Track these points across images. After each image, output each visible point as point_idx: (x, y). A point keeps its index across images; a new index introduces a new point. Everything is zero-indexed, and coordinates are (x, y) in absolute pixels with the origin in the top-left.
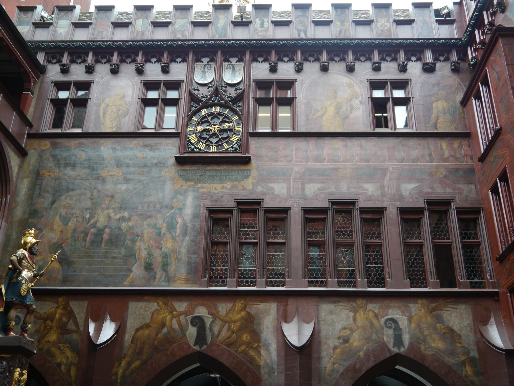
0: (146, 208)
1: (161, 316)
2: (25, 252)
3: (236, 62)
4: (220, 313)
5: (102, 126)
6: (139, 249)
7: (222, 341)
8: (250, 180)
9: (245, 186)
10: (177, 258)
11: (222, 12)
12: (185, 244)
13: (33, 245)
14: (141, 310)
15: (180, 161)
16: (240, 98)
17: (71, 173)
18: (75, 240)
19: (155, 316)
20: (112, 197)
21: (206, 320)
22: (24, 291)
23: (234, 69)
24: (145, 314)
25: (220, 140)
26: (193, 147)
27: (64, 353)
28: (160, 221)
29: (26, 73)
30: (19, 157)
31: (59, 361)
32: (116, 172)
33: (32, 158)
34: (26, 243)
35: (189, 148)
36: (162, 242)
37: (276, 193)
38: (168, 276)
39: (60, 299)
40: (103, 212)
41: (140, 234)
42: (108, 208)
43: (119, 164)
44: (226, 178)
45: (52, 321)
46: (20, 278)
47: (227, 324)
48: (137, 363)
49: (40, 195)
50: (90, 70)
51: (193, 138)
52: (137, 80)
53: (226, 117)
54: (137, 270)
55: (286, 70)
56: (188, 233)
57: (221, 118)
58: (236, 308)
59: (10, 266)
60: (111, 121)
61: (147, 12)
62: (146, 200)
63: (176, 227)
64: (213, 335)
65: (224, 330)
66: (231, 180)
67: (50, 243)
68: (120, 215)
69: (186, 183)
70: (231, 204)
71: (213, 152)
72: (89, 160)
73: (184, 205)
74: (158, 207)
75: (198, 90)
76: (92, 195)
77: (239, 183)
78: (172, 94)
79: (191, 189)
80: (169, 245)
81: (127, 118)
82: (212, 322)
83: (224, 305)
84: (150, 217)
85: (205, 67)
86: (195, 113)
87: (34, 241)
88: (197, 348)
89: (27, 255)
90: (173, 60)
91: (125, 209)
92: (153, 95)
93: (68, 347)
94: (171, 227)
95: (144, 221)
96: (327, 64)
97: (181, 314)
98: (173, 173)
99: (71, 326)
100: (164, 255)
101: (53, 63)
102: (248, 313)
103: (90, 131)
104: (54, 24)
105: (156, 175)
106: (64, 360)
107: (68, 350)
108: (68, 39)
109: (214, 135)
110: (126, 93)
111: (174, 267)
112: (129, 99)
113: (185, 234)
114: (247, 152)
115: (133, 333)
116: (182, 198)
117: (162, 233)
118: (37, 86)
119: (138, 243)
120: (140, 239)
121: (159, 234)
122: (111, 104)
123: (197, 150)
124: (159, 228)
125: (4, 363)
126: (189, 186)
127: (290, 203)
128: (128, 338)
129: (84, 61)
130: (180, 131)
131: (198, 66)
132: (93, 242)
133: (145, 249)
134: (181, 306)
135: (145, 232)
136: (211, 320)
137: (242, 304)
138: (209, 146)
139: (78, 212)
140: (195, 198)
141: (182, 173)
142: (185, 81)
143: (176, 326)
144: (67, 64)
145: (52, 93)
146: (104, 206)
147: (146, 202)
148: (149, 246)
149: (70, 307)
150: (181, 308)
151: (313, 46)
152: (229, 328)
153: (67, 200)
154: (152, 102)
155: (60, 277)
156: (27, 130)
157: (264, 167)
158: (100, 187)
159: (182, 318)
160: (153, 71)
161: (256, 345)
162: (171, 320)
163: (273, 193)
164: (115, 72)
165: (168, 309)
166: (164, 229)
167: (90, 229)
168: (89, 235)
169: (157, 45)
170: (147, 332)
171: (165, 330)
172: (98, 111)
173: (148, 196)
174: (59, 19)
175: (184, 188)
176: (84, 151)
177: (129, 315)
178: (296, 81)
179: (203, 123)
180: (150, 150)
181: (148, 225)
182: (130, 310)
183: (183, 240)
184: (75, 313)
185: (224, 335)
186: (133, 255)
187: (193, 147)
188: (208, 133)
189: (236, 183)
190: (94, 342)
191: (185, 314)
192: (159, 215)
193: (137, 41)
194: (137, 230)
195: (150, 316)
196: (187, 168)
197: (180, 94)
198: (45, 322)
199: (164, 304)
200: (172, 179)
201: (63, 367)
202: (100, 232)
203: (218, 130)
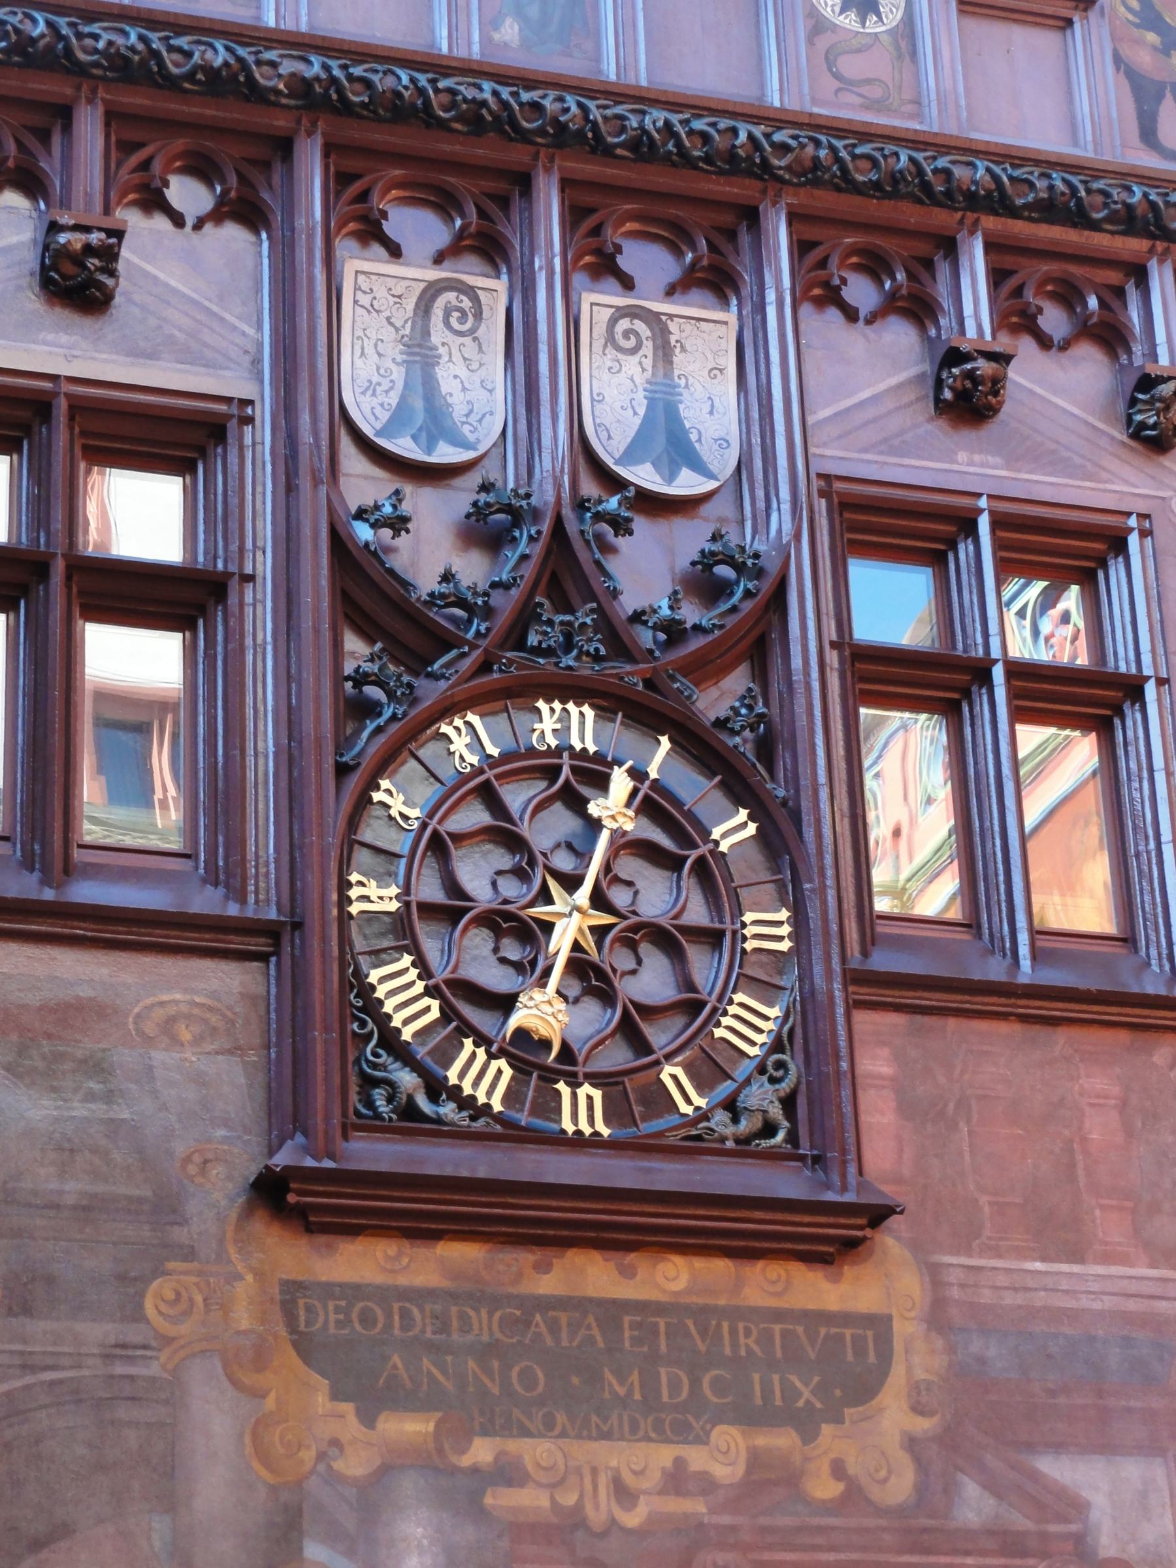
8: (893, 1416)
26: (407, 1079)
35: (369, 1083)
37: (1107, 1546)
69: (368, 1419)
71: (578, 1142)
77: (809, 1435)
98: (243, 1318)
123: (448, 1110)
142: (264, 413)
157: (986, 1296)
163: (1081, 1545)
175: (355, 1465)
189: (783, 1440)
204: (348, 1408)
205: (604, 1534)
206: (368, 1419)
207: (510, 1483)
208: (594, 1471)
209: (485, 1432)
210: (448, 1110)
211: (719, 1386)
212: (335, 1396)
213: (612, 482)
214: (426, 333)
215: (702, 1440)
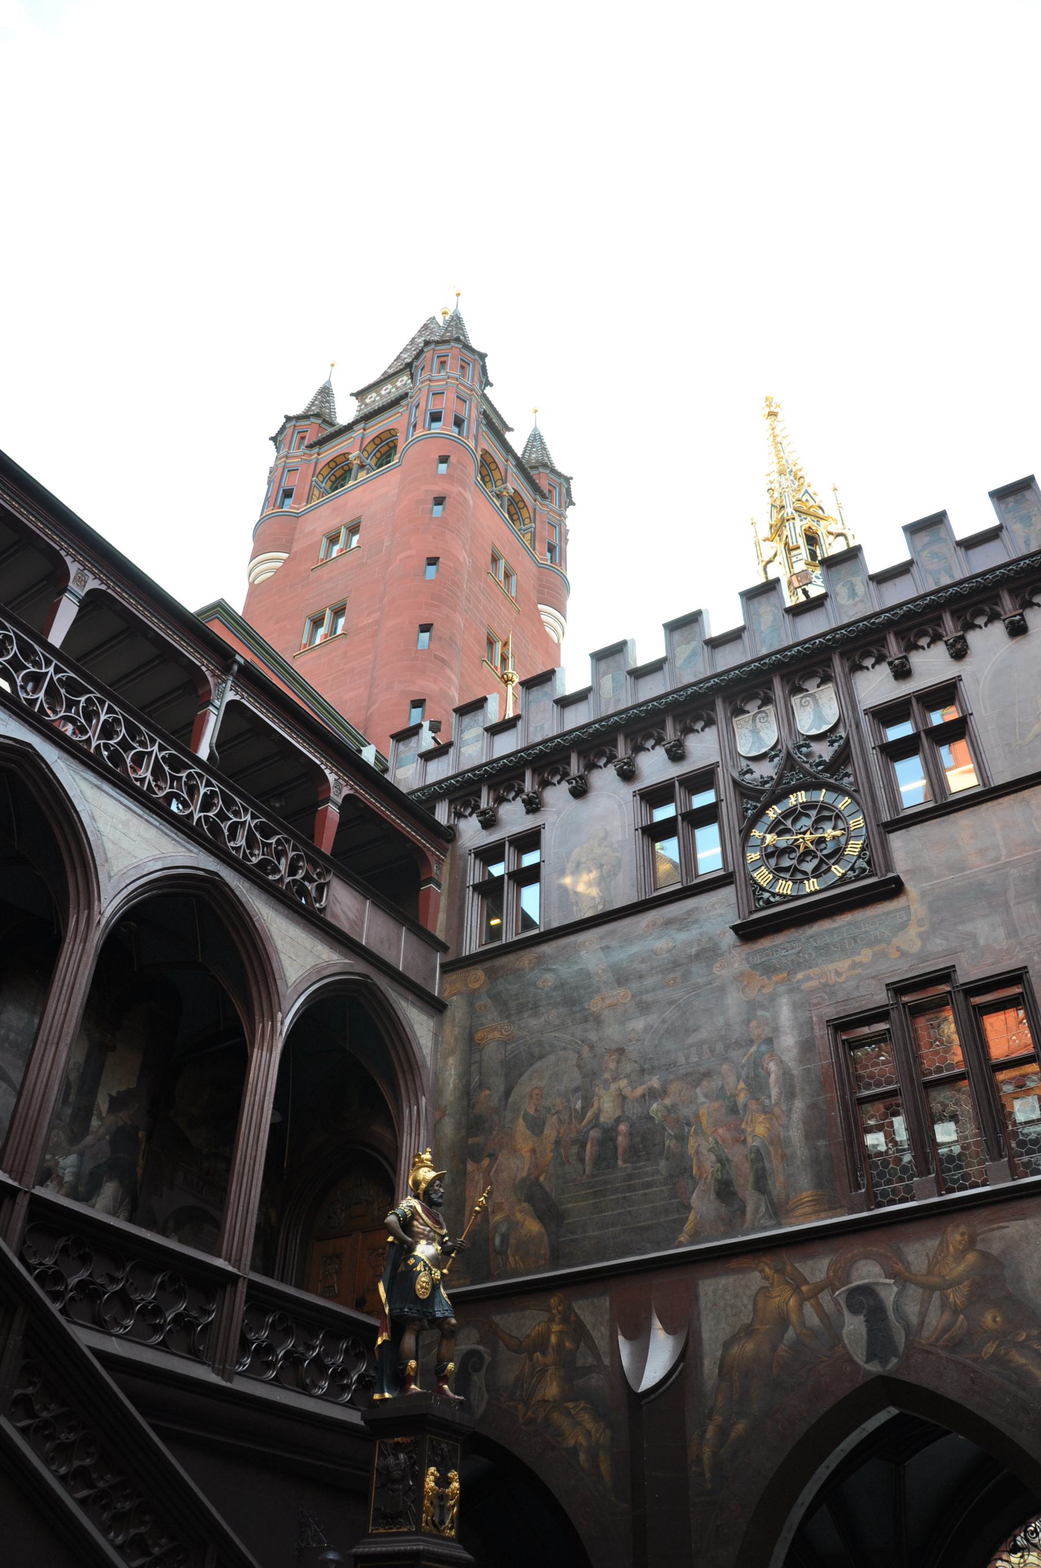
2: (415, 1203)
4: (914, 1269)
5: (575, 908)
6: (697, 1153)
7: (933, 1339)
8: (913, 932)
9: (904, 947)
10: (784, 1156)
11: (763, 599)
12: (796, 1116)
13: (431, 1183)
14: (728, 1297)
15: (748, 932)
16: (843, 757)
17: (533, 1022)
18: (562, 1164)
20: (621, 1051)
21: (883, 1293)
22: (422, 1288)
23: (816, 702)
25: (822, 862)
26: (766, 895)
27: (579, 1424)
28: (731, 1079)
29: (418, 850)
30: (431, 1016)
31: (572, 1442)
32: (620, 994)
33: (457, 1009)
34: (417, 1183)
35: (759, 899)
38: (772, 1203)
39: (553, 1301)
40: (607, 1088)
41: (692, 1120)
42: (615, 1079)
44: (855, 942)
45: (544, 1353)
46: (412, 1261)
47: (937, 1294)
48: (740, 1427)
49: (481, 1086)
50: (533, 806)
51: (763, 876)
52: (626, 792)
54: (702, 1204)
55: (932, 665)
56: (797, 1090)
57: (813, 813)
58: (951, 1248)
59: (390, 1239)
61: (617, 657)
62: (690, 1041)
63: (768, 1084)
64: (907, 1327)
65: (931, 1308)
66: (871, 944)
67: (514, 1180)
68: (644, 1086)
69: (770, 979)
70: (881, 997)
71: (812, 894)
72: (562, 985)
73: (776, 1030)
74: (719, 1047)
75: (750, 771)
76: (580, 1057)
77: (889, 943)
78: (703, 799)
79: (782, 989)
80: (761, 1130)
81: (620, 877)
82: (899, 1294)
83: (917, 1246)
84: (707, 1074)
85: (754, 720)
86: (754, 822)
87: (433, 1174)
88: (874, 1368)
89: (419, 1208)
90: (688, 730)
91: (653, 1070)
92: (664, 813)
93: (585, 1408)
94: (757, 1084)
95: (695, 1087)
96: (1018, 617)
97: (819, 1289)
100: (753, 1155)
101: (466, 817)
102: (985, 1256)
104: (455, 743)
105: (701, 981)
106: (581, 1439)
107: (586, 1416)
109: (808, 852)
110: (608, 828)
111: (782, 1179)
112: (617, 837)
113: (790, 1094)
114: (889, 867)
115: (719, 1354)
116: (767, 1014)
117: (740, 1105)
118: (446, 868)
119: (692, 1142)
121: (733, 1110)
122: (584, 859)
123: (777, 898)
126: (776, 983)
127: (1022, 956)
128: (709, 1366)
129: (521, 791)
130: (731, 869)
132: (598, 1160)
133: (710, 1150)
134: (817, 1268)
135: (703, 1111)
136: (895, 1289)
137: (963, 1234)
138: (801, 881)
139: (558, 1101)
140: (796, 1007)
143: (813, 1319)
144: (491, 809)
145: (475, 874)
146: (607, 1075)
147: (691, 1046)
148: (717, 1142)
149: (577, 1316)
150: (817, 1273)
151: (975, 591)
152: (944, 1304)
153: (534, 1082)
155: (545, 1250)
158: (592, 1036)
159: (825, 1297)
160: (654, 766)
161: (1023, 1336)
164: (580, 792)
165: (788, 1283)
166: (742, 1095)
167: (588, 1132)
168: (589, 1146)
170: (750, 1346)
171: (790, 1334)
173: (694, 1031)
176: (550, 970)
177: (703, 1313)
178: (959, 678)
181: (706, 1096)
182: (703, 1300)
183: (790, 1110)
184: (588, 1327)
185: (934, 1323)
187: (766, 895)
188: (792, 856)
190: (634, 1388)
191: (830, 1285)
192: (725, 1067)
193: (608, 718)
194: (686, 1111)
195: (750, 1307)
196: (766, 943)
197: (718, 794)
198: (531, 1360)
199: (777, 1271)
201: (582, 1457)
202: (609, 1135)
203: (812, 843)
206: (770, 979)
211: (862, 939)
212: (762, 975)
215: (859, 954)
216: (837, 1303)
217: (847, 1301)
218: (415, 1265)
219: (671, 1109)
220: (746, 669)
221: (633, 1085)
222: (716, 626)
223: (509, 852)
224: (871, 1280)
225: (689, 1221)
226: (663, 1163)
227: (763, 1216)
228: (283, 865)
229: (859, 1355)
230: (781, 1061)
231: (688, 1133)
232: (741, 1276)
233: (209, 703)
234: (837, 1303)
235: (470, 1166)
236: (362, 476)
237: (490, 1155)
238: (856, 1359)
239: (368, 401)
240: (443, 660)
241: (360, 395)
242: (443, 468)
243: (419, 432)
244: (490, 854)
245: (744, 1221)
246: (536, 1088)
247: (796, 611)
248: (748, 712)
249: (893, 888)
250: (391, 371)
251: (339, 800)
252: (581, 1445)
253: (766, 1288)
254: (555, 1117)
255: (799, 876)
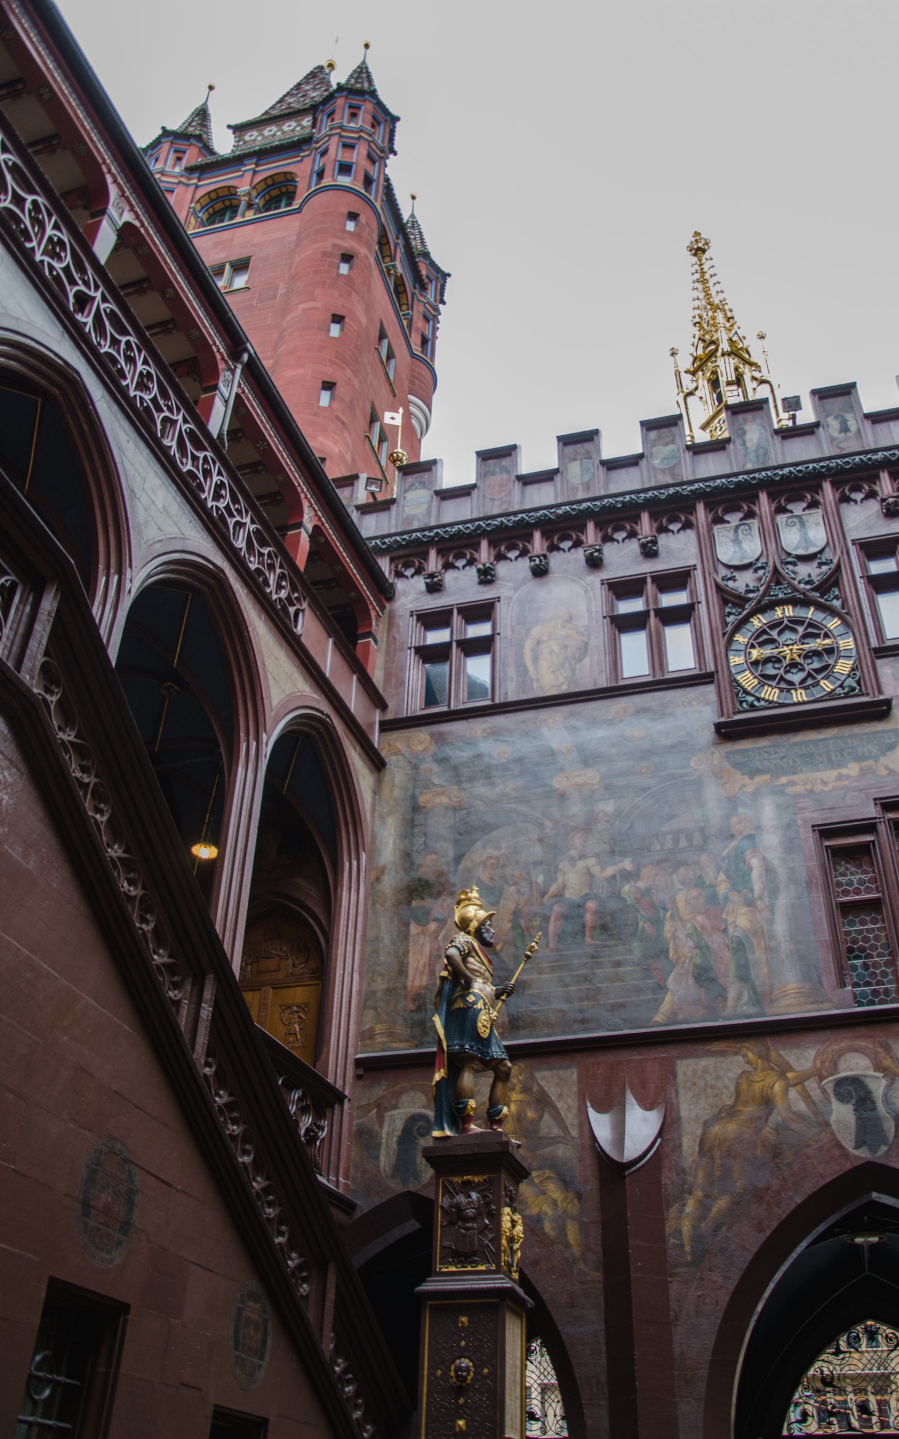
0: (669, 845)
1: (757, 1087)
3: (804, 510)
5: (535, 685)
6: (674, 937)
9: (891, 766)
13: (482, 923)
15: (728, 732)
16: (832, 582)
19: (744, 1087)
22: (484, 1026)
23: (803, 524)
24: (720, 1085)
25: (809, 675)
26: (750, 699)
29: (362, 600)
31: (535, 1211)
35: (741, 702)
36: (724, 916)
38: (755, 993)
41: (669, 906)
42: (583, 857)
43: (588, 759)
44: (842, 755)
46: (471, 998)
48: (722, 1203)
50: (487, 577)
51: (747, 680)
53: (810, 625)
57: (801, 629)
60: (553, 672)
61: (588, 446)
62: (665, 829)
66: (858, 759)
69: (752, 778)
70: (871, 811)
71: (799, 704)
74: (697, 838)
75: (733, 578)
77: (876, 761)
80: (743, 921)
81: (587, 661)
82: (889, 1087)
84: (685, 864)
86: (738, 628)
88: (863, 1154)
91: (623, 854)
99: (548, 1127)
101: (407, 577)
103: (511, 698)
106: (547, 1208)
108: (433, 523)
109: (794, 665)
114: (880, 692)
115: (699, 1132)
119: (668, 927)
120: (671, 915)
121: (713, 899)
122: (545, 638)
123: (763, 703)
124: (711, 886)
125: (474, 1195)
128: (689, 1144)
130: (711, 668)
131: (722, 534)
133: (688, 936)
134: (803, 1056)
135: (680, 897)
136: (884, 1082)
138: (788, 691)
141: (739, 758)
143: (801, 1106)
144: (440, 573)
146: (573, 853)
148: (695, 929)
154: (634, 623)
156: (377, 716)
160: (622, 558)
162: (785, 1092)
164: (540, 572)
165: (772, 1069)
168: (552, 919)
169: (623, 502)
170: (731, 1128)
171: (776, 1117)
172: (520, 657)
174: (406, 491)
175: (750, 789)
176: (505, 741)
179: (761, 645)
180: (653, 720)
181: (683, 883)
182: (680, 1077)
186: (663, 952)
187: (750, 699)
188: (777, 665)
189: (870, 762)
192: (704, 858)
194: (660, 897)
195: (732, 1089)
199: (760, 1057)
200: (718, 774)
203: (799, 656)
204: (746, 777)
205: (820, 793)
207: (792, 786)
208: (816, 780)
209: (784, 776)
210: (763, 703)
211: (849, 754)
212: (743, 774)
213: (789, 554)
214: (738, 537)
215: (846, 767)
216: (824, 1091)
217: (835, 1090)
218: (475, 1003)
219: (646, 892)
220: (735, 480)
221: (603, 865)
222: (611, 447)
223: (456, 619)
224: (860, 1072)
225: (666, 1002)
226: (636, 945)
227: (746, 1004)
228: (272, 580)
229: (848, 1141)
230: (764, 858)
231: (664, 917)
232: (722, 1059)
233: (215, 387)
234: (824, 1091)
235: (414, 929)
236: (250, 215)
237: (436, 920)
238: (844, 1144)
239: (247, 138)
240: (343, 423)
241: (239, 129)
242: (350, 226)
243: (326, 181)
244: (432, 620)
245: (725, 1007)
246: (491, 858)
247: (786, 434)
248: (728, 522)
249: (880, 711)
250: (275, 112)
251: (310, 527)
252: (546, 1214)
253: (749, 1072)
254: (513, 888)
255: (783, 685)
